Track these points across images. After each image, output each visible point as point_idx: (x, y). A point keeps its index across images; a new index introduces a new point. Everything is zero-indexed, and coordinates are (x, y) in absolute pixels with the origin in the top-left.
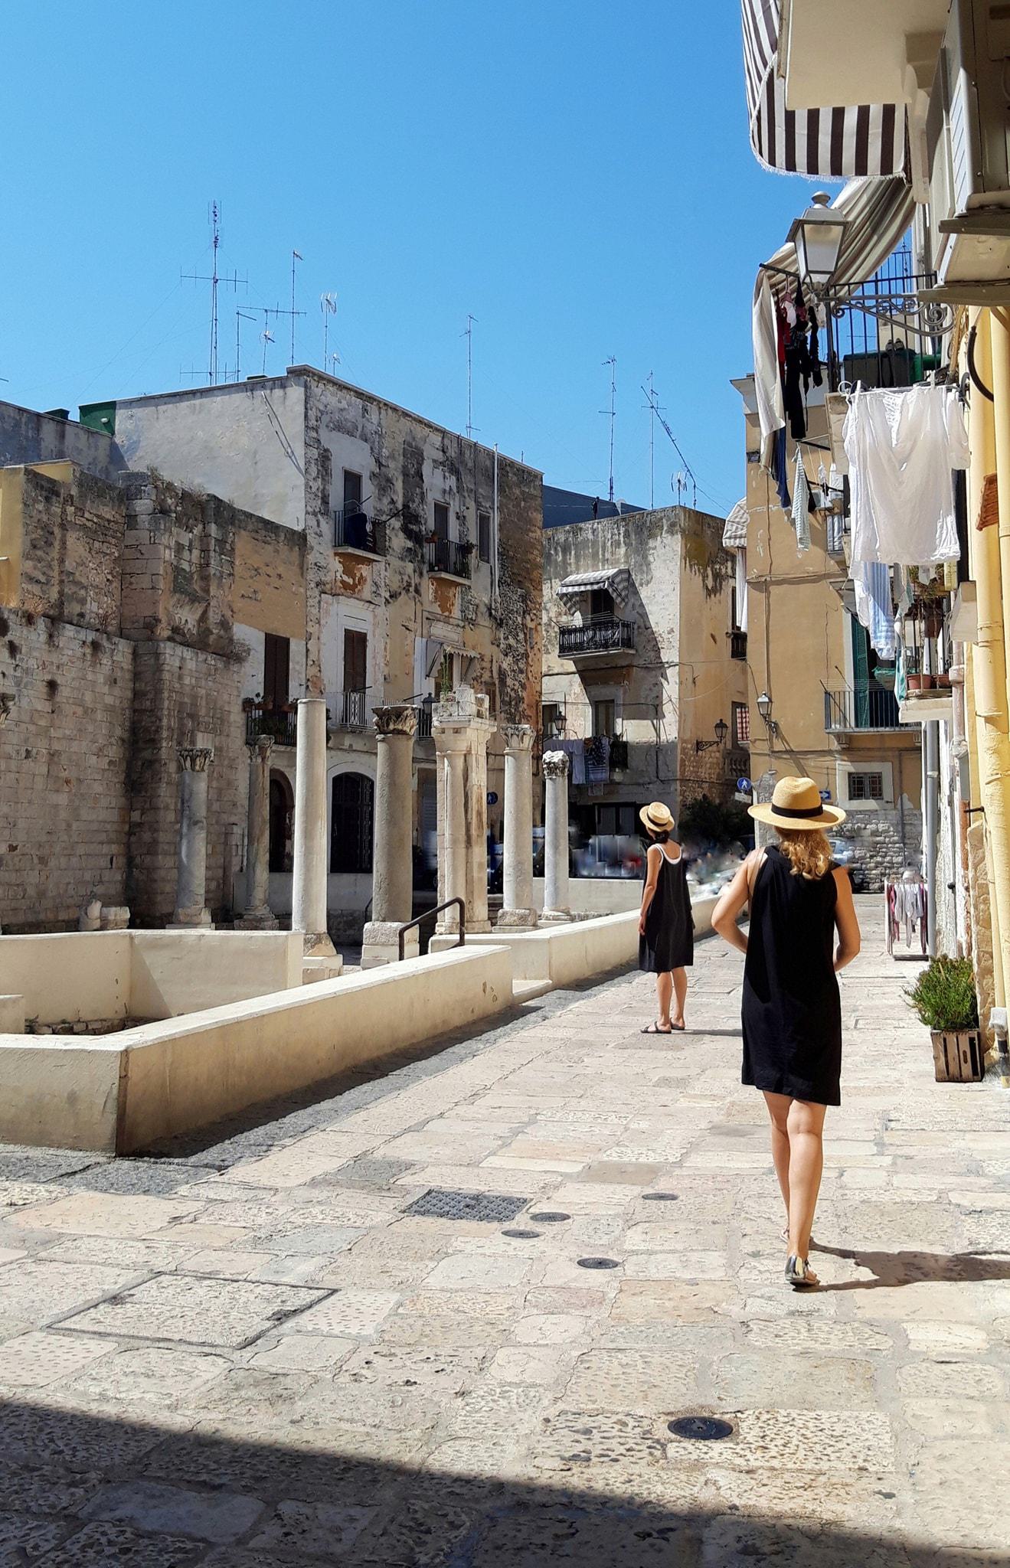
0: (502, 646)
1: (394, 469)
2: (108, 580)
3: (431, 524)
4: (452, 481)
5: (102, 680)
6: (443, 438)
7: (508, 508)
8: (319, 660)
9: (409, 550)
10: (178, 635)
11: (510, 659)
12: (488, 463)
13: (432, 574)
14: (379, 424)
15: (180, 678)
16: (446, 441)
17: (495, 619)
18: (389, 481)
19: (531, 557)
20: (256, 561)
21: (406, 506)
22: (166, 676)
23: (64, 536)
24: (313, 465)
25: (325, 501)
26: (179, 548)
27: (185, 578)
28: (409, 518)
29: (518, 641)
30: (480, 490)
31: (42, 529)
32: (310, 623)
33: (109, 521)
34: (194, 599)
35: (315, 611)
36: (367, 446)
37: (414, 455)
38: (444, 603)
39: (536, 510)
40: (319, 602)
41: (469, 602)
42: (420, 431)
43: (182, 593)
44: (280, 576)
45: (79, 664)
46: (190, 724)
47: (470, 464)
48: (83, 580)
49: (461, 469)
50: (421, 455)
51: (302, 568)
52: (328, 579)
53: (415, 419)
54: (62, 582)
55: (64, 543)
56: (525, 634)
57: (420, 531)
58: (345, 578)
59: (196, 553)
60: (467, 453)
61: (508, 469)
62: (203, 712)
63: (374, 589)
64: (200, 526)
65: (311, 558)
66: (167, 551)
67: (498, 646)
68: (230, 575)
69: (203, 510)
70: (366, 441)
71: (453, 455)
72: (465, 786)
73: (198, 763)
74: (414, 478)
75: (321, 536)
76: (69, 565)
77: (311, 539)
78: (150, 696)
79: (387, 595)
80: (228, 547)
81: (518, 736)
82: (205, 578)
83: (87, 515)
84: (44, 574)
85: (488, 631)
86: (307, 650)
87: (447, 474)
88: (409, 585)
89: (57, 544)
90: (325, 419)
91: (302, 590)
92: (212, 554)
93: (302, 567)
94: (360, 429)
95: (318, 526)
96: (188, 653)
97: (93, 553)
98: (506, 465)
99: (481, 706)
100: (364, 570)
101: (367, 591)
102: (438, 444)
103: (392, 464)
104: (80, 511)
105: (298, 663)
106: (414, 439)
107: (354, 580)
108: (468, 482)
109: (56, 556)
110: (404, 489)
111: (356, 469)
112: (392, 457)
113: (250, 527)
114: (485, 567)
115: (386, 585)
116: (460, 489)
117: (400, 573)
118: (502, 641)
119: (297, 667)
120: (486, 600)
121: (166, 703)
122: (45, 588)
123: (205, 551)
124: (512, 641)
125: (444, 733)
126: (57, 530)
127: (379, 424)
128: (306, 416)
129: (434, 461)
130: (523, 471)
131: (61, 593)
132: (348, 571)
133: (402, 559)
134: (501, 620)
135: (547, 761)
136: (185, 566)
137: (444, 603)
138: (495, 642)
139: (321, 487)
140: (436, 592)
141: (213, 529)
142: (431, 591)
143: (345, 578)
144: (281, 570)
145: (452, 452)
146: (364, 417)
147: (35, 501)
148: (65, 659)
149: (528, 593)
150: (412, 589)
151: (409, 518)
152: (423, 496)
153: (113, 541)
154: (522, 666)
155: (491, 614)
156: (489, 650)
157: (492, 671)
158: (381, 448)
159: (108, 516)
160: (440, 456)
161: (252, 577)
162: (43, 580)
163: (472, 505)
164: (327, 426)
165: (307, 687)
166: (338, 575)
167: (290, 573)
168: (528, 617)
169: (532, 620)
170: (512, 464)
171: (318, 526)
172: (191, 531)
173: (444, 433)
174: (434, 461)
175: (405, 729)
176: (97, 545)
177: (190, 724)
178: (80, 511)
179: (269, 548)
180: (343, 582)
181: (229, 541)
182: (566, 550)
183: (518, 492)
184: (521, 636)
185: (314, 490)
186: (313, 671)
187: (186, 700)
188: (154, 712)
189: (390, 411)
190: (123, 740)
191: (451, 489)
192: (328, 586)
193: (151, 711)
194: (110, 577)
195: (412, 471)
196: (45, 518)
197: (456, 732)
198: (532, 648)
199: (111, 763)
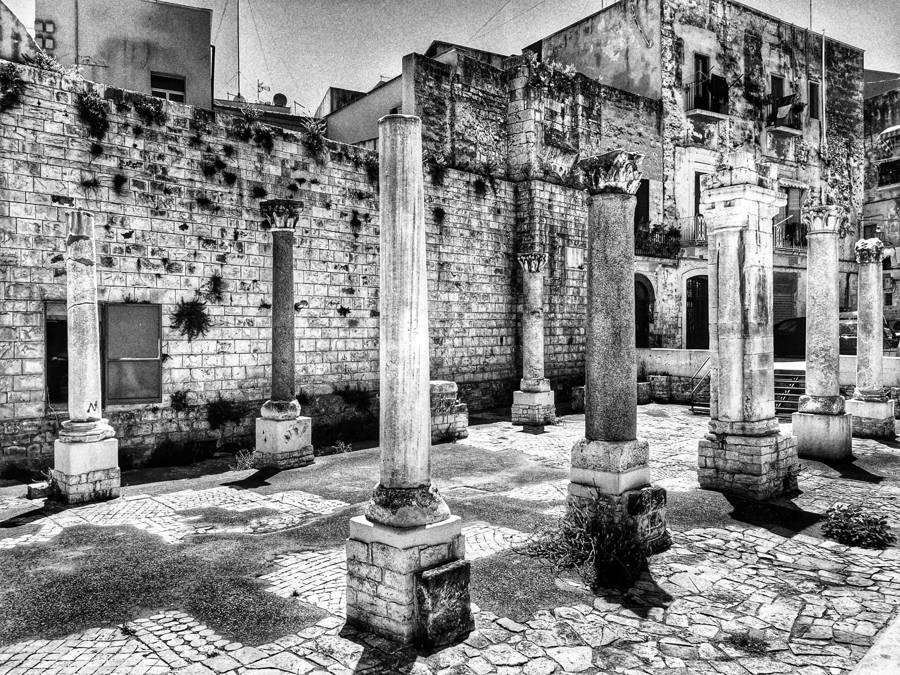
0: (829, 180)
1: (736, 51)
2: (496, 140)
3: (769, 91)
4: (786, 59)
5: (486, 211)
6: (778, 27)
7: (835, 79)
8: (674, 195)
9: (750, 111)
10: (548, 176)
11: (836, 190)
12: (817, 44)
13: (770, 128)
14: (724, 18)
15: (550, 207)
16: (781, 30)
17: (823, 160)
18: (733, 60)
19: (854, 114)
20: (619, 123)
21: (747, 78)
22: (537, 206)
23: (453, 106)
24: (668, 51)
25: (678, 76)
26: (553, 114)
27: (558, 136)
28: (750, 87)
29: (843, 177)
30: (811, 65)
31: (434, 100)
32: (666, 169)
33: (494, 96)
34: (566, 151)
35: (670, 159)
36: (714, 35)
37: (754, 39)
38: (780, 149)
39: (858, 78)
40: (674, 153)
41: (802, 148)
42: (758, 22)
43: (553, 146)
44: (640, 134)
45: (464, 199)
46: (560, 242)
47: (802, 46)
48: (472, 139)
49: (794, 50)
50: (760, 40)
51: (659, 128)
52: (681, 135)
53: (754, 13)
54: (453, 141)
55: (453, 111)
56: (849, 172)
57: (760, 96)
58: (696, 134)
59: (568, 118)
60: (800, 37)
61: (834, 48)
62: (573, 232)
63: (720, 141)
64: (571, 98)
65: (667, 121)
66: (538, 114)
67: (826, 180)
68: (596, 134)
69: (573, 85)
70: (713, 30)
71: (787, 39)
72: (741, 267)
73: (533, 265)
74: (754, 59)
75: (675, 103)
76: (458, 127)
77: (667, 106)
78: (527, 222)
79: (731, 145)
80: (594, 112)
81: (821, 218)
82: (576, 136)
83: (472, 90)
84: (437, 134)
85: (817, 169)
86: (664, 188)
87: (782, 54)
88: (750, 137)
89: (448, 112)
90: (679, 15)
91: (659, 144)
92: (580, 117)
93: (659, 128)
94: (707, 22)
95: (673, 96)
96: (557, 190)
97: (480, 119)
98: (832, 46)
99: (765, 174)
100: (712, 128)
101: (715, 141)
102: (774, 32)
103: (735, 47)
104: (467, 87)
105: (656, 198)
106: (754, 28)
107: (703, 135)
108: (800, 59)
109: (447, 120)
110: (745, 65)
111: (705, 52)
112: (735, 41)
113: (614, 98)
114: (815, 123)
115: (731, 138)
116: (793, 65)
117: (742, 129)
118: (830, 177)
119: (656, 201)
120: (816, 146)
121: (538, 226)
122: (438, 144)
123: (574, 115)
124: (838, 177)
125: (713, 208)
126: (447, 102)
127: (724, 18)
128: (662, 14)
129: (771, 44)
130: (847, 50)
131: (453, 148)
132: (699, 129)
133: (744, 118)
134: (829, 161)
135: (860, 248)
136: (558, 127)
137: (780, 149)
138: (824, 178)
139: (675, 67)
140: (773, 142)
141: (580, 99)
142: (769, 141)
143: (696, 134)
144: (641, 129)
145: (786, 37)
146: (710, 12)
147: (426, 79)
148: (450, 195)
149: (851, 140)
150: (753, 140)
151: (750, 87)
152: (761, 70)
153: (498, 111)
154: (846, 195)
155: (820, 157)
156: (818, 184)
157: (821, 200)
158: (725, 35)
159: (492, 92)
160: (775, 40)
161: (616, 136)
162: (437, 138)
163: (804, 76)
164: (680, 21)
165: (665, 215)
166: (690, 132)
167: (650, 134)
168: (851, 159)
169: (855, 161)
170: (838, 44)
171: (673, 96)
172: (563, 101)
173: (779, 23)
174: (771, 44)
175: (620, 185)
176: (483, 113)
177: (560, 242)
178: (467, 87)
179: (631, 114)
180: (693, 137)
181: (596, 108)
182: (884, 110)
183: (842, 65)
184: (846, 173)
185: (669, 69)
186: (669, 203)
187: (556, 224)
188: (529, 232)
189: (733, 7)
190: (506, 254)
191: (785, 65)
192: (681, 141)
193: (529, 232)
194: (497, 138)
195: (752, 52)
196: (436, 93)
197: (729, 206)
198: (855, 182)
199: (497, 271)
